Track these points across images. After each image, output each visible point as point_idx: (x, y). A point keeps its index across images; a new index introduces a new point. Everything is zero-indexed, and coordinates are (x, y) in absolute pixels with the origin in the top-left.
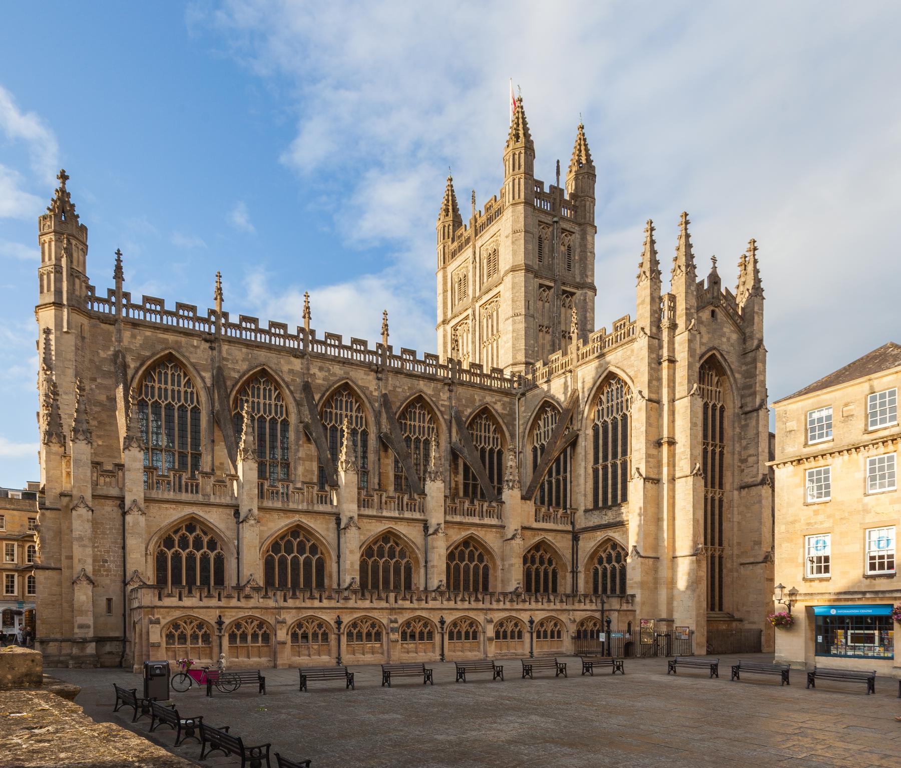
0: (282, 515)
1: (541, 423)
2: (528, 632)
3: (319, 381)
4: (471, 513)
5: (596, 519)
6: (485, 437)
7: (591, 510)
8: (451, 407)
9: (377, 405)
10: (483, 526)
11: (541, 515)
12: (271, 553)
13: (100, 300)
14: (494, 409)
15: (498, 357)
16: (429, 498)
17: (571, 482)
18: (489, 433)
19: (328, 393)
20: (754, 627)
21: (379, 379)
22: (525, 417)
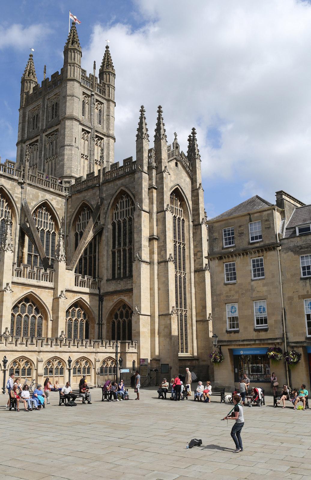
1: (81, 217)
2: (67, 369)
5: (113, 287)
6: (44, 222)
11: (79, 282)
14: (50, 203)
15: (55, 170)
17: (98, 260)
18: (47, 220)
20: (204, 363)
22: (71, 212)
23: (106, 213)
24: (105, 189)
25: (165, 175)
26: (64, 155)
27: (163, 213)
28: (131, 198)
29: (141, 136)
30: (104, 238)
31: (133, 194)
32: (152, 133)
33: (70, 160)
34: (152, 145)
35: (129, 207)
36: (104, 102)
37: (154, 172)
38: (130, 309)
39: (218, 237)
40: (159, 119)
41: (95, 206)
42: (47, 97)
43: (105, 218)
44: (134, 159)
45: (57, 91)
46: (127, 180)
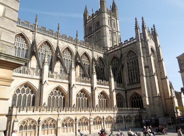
0: (54, 83)
3: (61, 46)
4: (103, 85)
7: (129, 84)
9: (75, 54)
10: (105, 88)
12: (50, 95)
16: (92, 80)
19: (63, 49)
21: (75, 47)
23: (124, 59)
24: (122, 50)
25: (148, 42)
27: (149, 57)
28: (134, 53)
29: (137, 28)
30: (124, 69)
31: (135, 51)
32: (141, 27)
33: (106, 41)
34: (141, 32)
35: (134, 56)
36: (115, 19)
37: (143, 42)
38: (139, 95)
39: (183, 63)
40: (143, 21)
41: (119, 58)
43: (124, 61)
44: (134, 38)
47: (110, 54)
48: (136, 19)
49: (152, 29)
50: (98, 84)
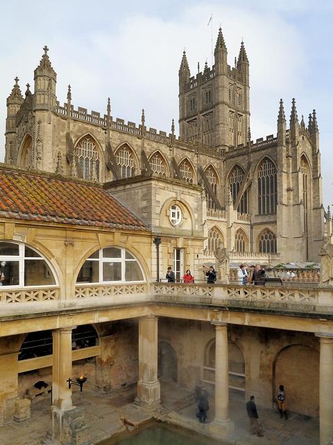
3: (148, 150)
5: (260, 220)
8: (198, 164)
10: (220, 221)
13: (61, 108)
23: (253, 172)
24: (252, 155)
26: (219, 131)
29: (281, 119)
30: (252, 188)
34: (288, 127)
36: (243, 87)
37: (290, 146)
40: (294, 108)
41: (245, 167)
42: (202, 87)
43: (253, 175)
44: (275, 136)
45: (210, 83)
46: (270, 150)
47: (228, 161)
48: (281, 103)
49: (310, 117)
50: (208, 215)
